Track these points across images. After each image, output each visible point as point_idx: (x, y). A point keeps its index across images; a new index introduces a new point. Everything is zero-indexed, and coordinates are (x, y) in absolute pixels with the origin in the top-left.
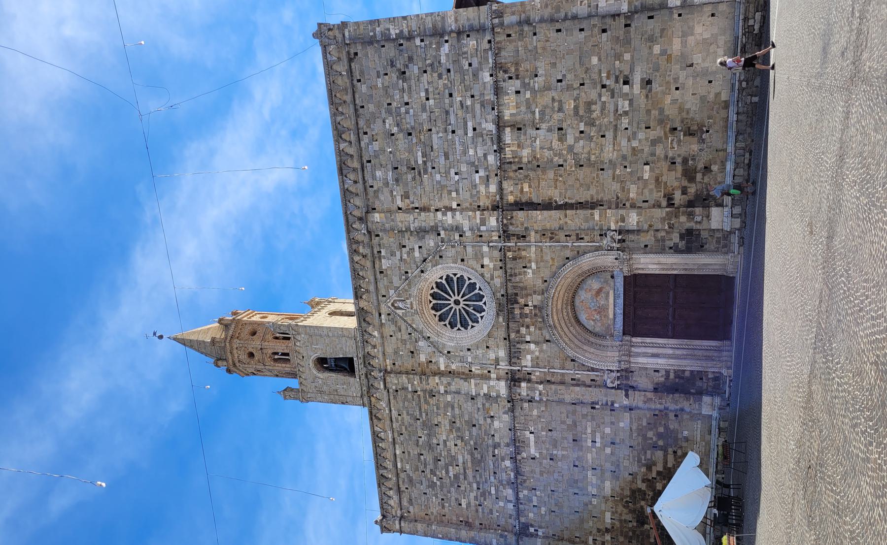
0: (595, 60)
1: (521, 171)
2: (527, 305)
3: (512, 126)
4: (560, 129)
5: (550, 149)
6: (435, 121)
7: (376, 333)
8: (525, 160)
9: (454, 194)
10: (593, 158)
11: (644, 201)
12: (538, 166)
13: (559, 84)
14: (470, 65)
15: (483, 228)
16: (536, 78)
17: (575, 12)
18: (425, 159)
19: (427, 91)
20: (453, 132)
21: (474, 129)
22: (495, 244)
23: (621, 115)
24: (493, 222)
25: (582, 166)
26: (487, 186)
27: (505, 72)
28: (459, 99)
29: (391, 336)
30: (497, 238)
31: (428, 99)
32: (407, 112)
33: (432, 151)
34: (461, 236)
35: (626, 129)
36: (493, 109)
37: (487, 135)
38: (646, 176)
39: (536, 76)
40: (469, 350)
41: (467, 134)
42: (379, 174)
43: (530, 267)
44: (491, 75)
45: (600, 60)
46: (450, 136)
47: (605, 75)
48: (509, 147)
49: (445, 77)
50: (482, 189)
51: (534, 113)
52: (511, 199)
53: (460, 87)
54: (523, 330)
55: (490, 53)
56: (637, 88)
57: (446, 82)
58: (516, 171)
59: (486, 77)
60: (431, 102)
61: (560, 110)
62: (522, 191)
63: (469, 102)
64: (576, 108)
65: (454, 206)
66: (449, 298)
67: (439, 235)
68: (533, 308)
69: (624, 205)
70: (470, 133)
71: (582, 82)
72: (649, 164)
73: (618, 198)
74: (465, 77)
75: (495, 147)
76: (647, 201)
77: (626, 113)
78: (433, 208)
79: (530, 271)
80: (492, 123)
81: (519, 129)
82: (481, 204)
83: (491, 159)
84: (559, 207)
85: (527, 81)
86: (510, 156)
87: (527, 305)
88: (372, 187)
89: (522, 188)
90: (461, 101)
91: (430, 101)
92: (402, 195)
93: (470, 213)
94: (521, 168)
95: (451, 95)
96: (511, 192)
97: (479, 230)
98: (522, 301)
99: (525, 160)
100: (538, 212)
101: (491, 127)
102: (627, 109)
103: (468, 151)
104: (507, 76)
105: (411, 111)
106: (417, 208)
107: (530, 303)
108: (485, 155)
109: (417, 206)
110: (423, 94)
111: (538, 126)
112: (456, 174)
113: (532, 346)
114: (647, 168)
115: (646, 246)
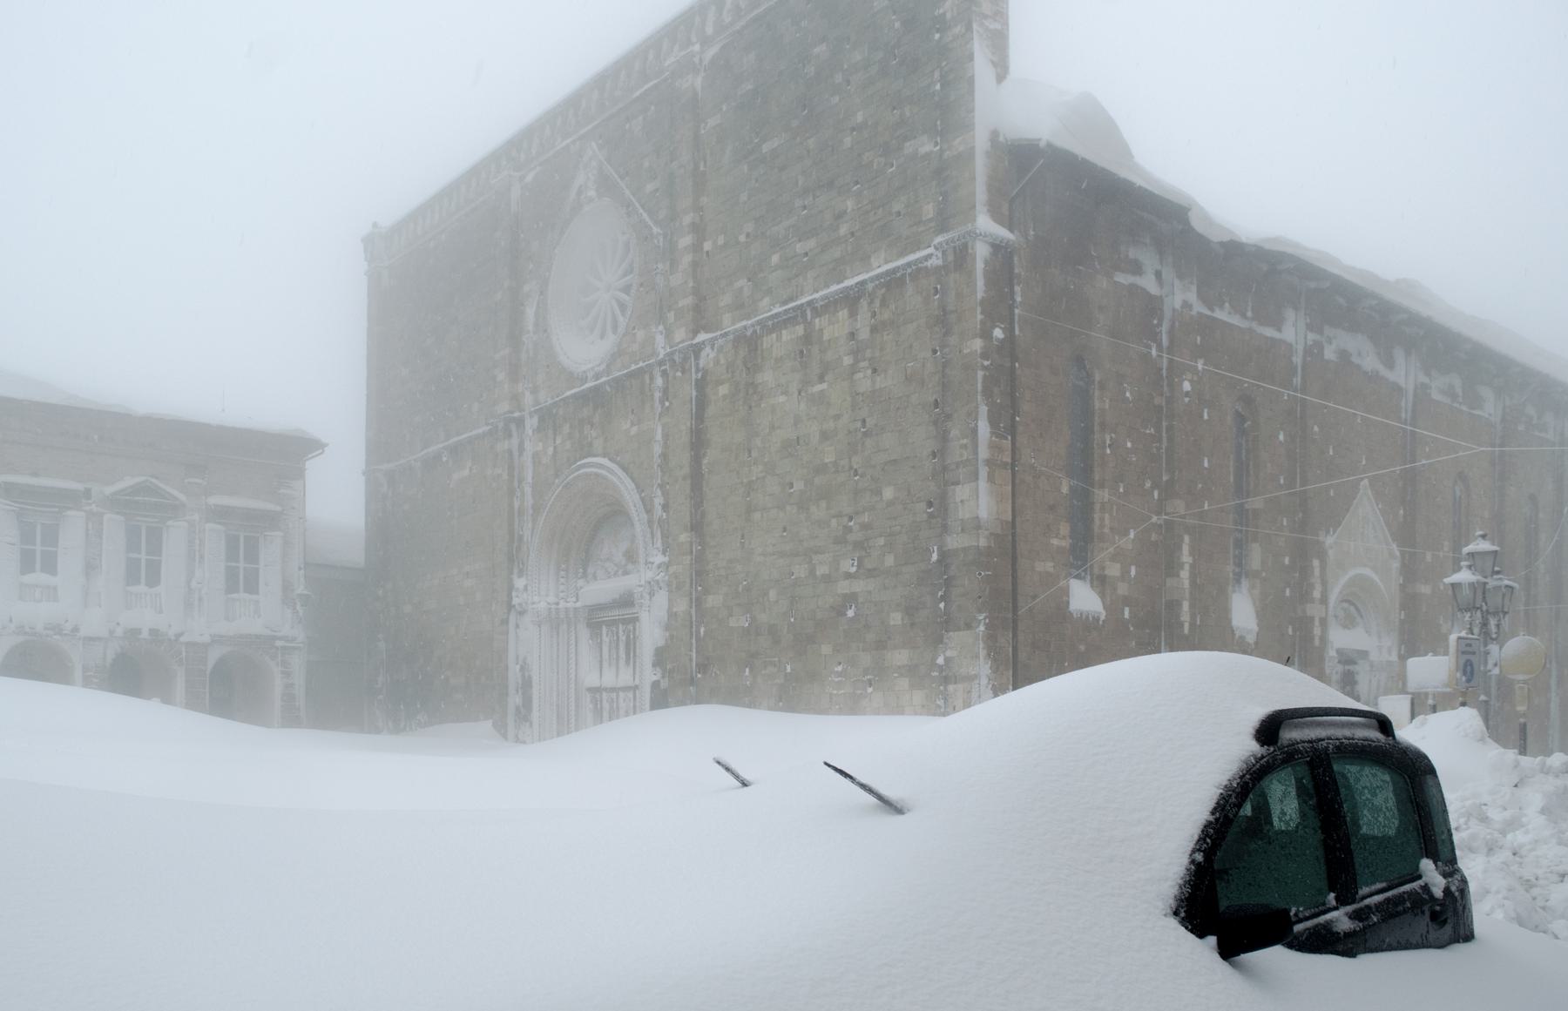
3: (807, 339)
5: (773, 428)
9: (721, 240)
10: (757, 516)
12: (750, 407)
16: (869, 372)
17: (951, 435)
37: (797, 286)
39: (875, 371)
43: (633, 424)
46: (798, 203)
48: (777, 340)
62: (720, 382)
65: (707, 246)
74: (881, 209)
84: (697, 460)
85: (868, 354)
90: (845, 212)
111: (803, 394)
113: (550, 451)
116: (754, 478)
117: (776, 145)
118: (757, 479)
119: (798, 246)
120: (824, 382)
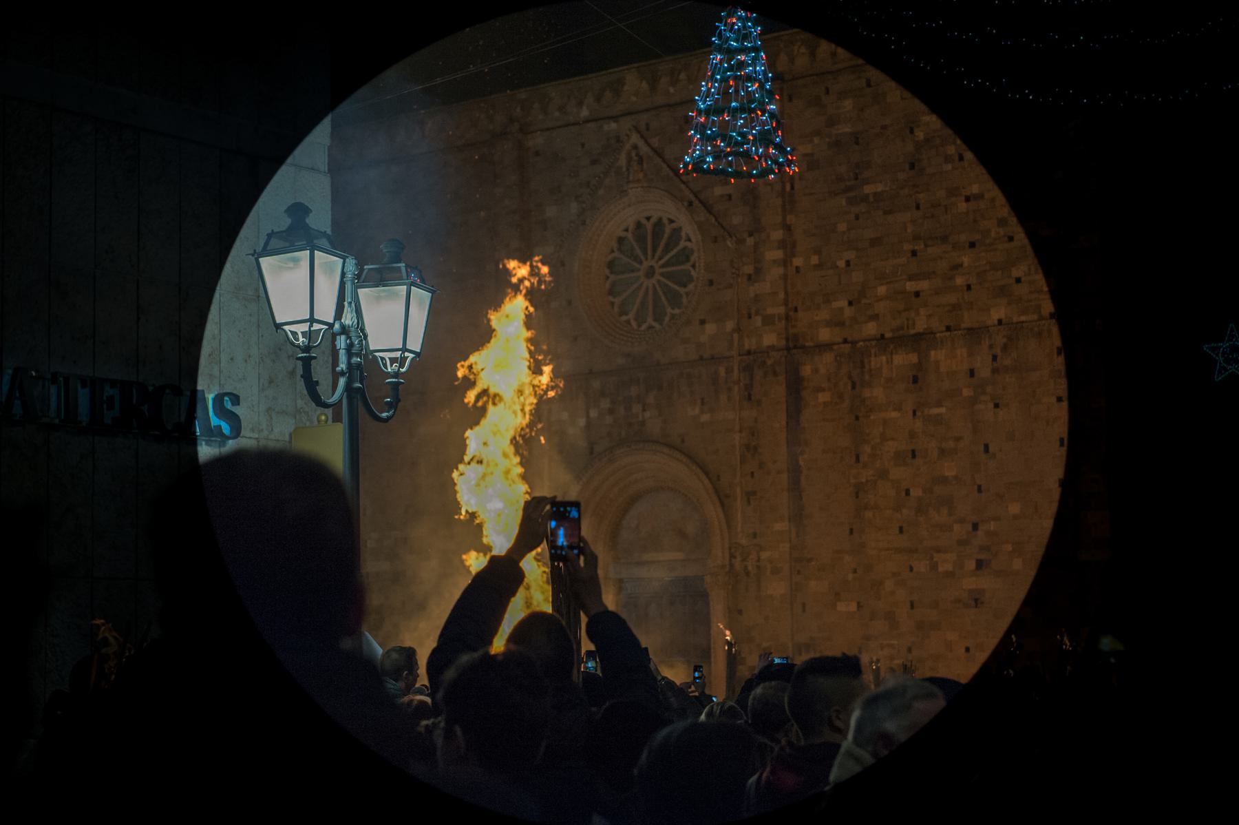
0: (1014, 509)
1: (850, 388)
2: (644, 410)
4: (914, 454)
6: (933, 216)
7: (585, 113)
8: (867, 393)
10: (869, 514)
11: (804, 605)
12: (857, 418)
13: (982, 448)
14: (1018, 280)
15: (758, 321)
16: (991, 405)
18: (871, 199)
19: (980, 196)
20: (914, 253)
21: (917, 294)
22: (736, 344)
23: (932, 558)
24: (769, 339)
25: (857, 497)
26: (828, 324)
27: (1005, 348)
28: (966, 260)
29: (583, 145)
30: (747, 347)
31: (968, 199)
32: (948, 159)
33: (886, 213)
34: (749, 277)
35: (911, 569)
36: (948, 329)
37: (908, 319)
38: (841, 607)
39: (996, 406)
40: (570, 303)
41: (911, 278)
42: (848, 104)
44: (1000, 322)
45: (1015, 517)
46: (907, 247)
47: (992, 528)
48: (888, 362)
49: (1002, 231)
50: (824, 315)
51: (939, 404)
52: (806, 370)
53: (984, 262)
54: (605, 404)
55: (1036, 317)
56: (970, 583)
57: (993, 234)
58: (850, 377)
59: (999, 312)
60: (963, 206)
61: (942, 452)
63: (959, 281)
64: (944, 480)
65: (798, 261)
66: (649, 257)
67: (751, 235)
68: (640, 419)
69: (799, 572)
70: (911, 286)
71: (983, 488)
72: (858, 610)
73: (810, 560)
74: (1000, 272)
75: (888, 335)
76: (804, 611)
77: (934, 567)
78: (790, 219)
79: (697, 411)
80: (926, 326)
81: (915, 380)
82: (800, 314)
83: (871, 329)
86: (873, 363)
87: (644, 410)
88: (827, 92)
89: (823, 390)
90: (961, 265)
91: (964, 204)
92: (812, 155)
93: (782, 295)
94: (854, 387)
95: (972, 245)
96: (816, 371)
97: (757, 313)
98: (651, 399)
99: (867, 393)
100: (784, 423)
101: (921, 325)
102: (940, 569)
103: (882, 284)
104: (998, 351)
105: (949, 167)
106: (792, 188)
107: (647, 414)
108: (875, 317)
109: (797, 186)
110: (975, 189)
111: (918, 414)
112: (848, 263)
113: (582, 422)
114: (853, 607)
115: (740, 612)
116: (864, 480)
117: (879, 190)
118: (867, 481)
119: (908, 284)
120: (942, 406)
